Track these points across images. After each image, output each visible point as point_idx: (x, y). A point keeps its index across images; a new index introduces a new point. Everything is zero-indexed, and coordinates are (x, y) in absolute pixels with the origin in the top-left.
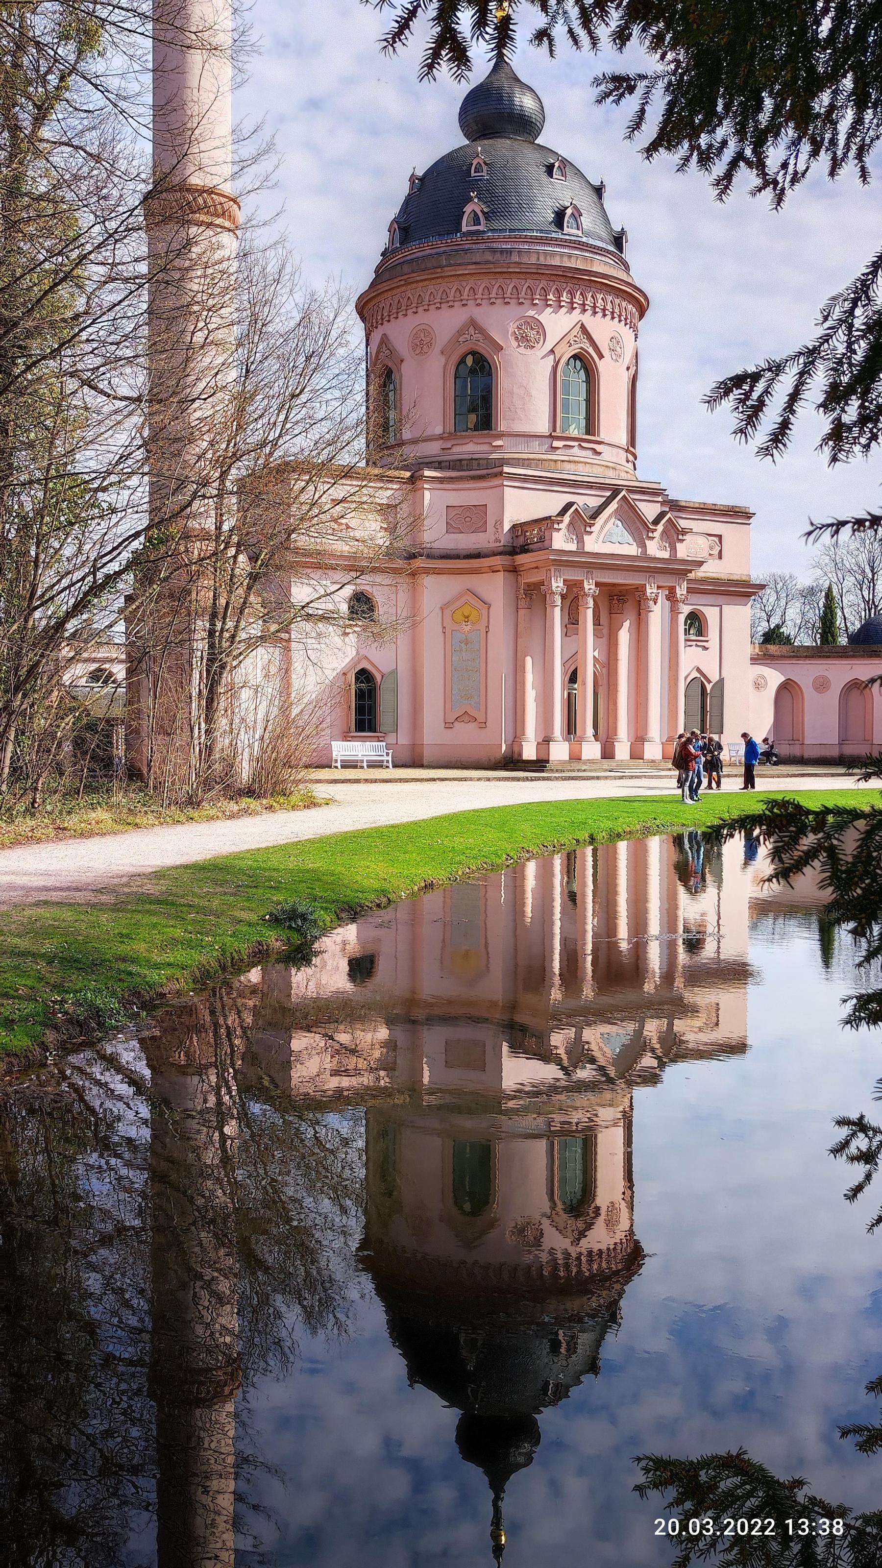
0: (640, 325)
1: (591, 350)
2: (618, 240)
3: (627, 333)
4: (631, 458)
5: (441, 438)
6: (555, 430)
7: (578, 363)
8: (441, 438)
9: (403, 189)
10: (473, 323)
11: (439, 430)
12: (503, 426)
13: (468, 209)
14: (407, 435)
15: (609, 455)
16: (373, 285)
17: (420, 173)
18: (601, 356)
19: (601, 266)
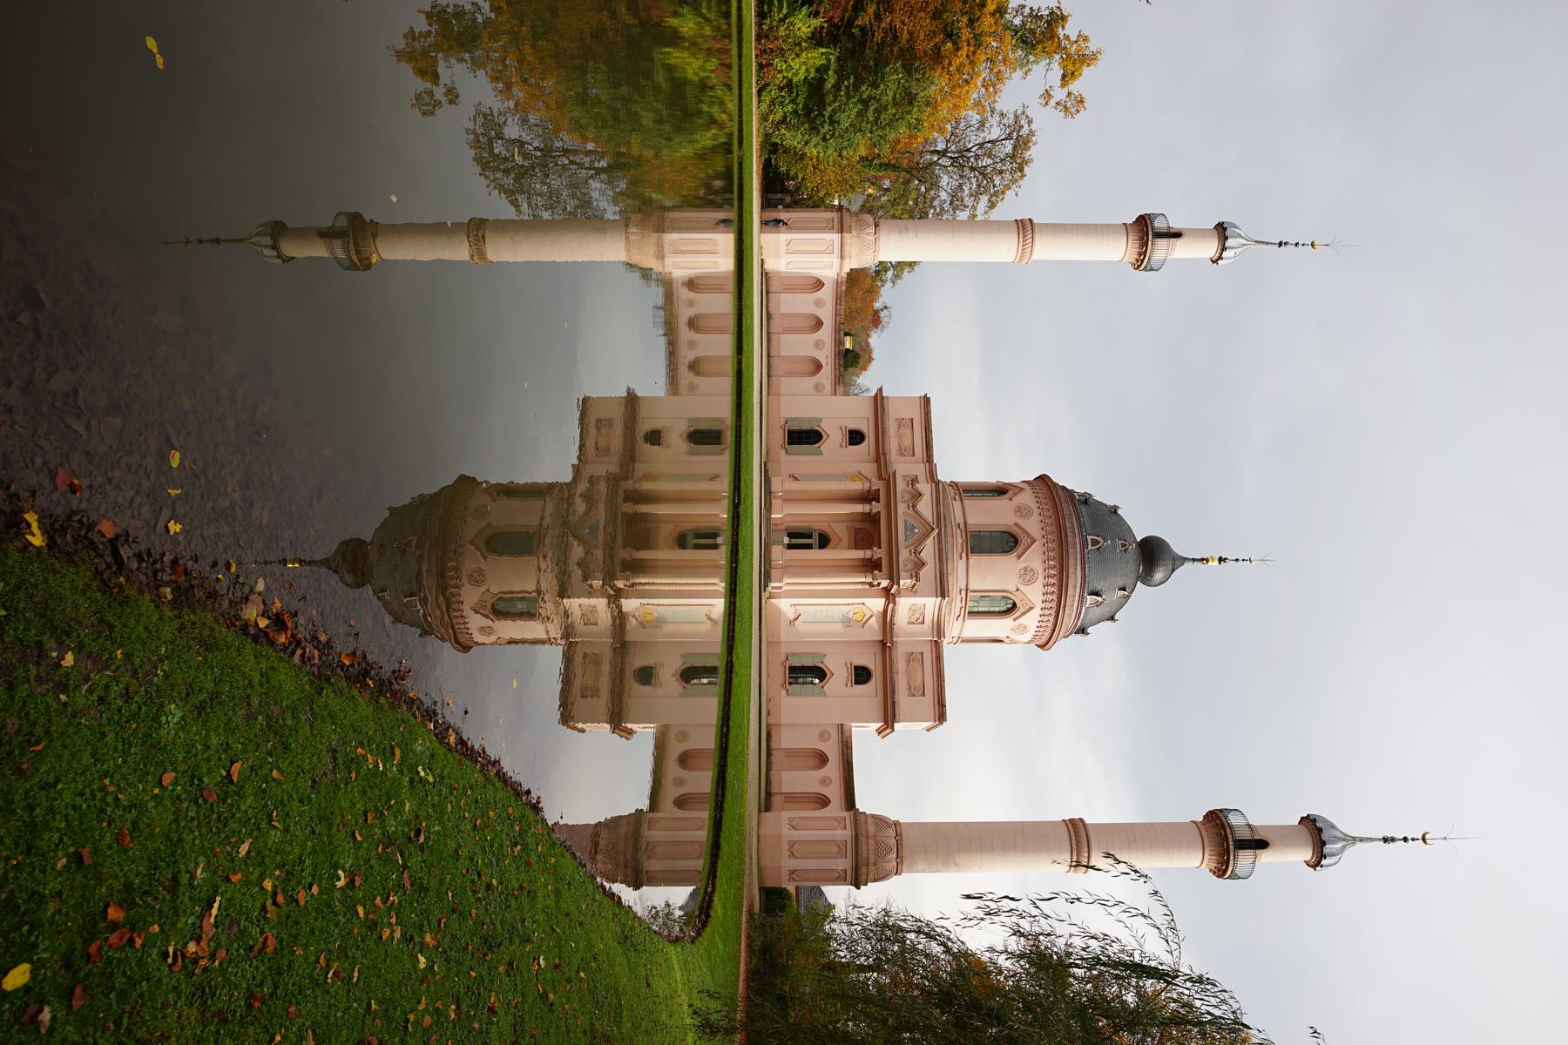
0: (1033, 645)
1: (1018, 614)
2: (1082, 631)
3: (1028, 636)
4: (955, 640)
5: (965, 523)
6: (972, 591)
7: (1010, 606)
8: (965, 523)
9: (1110, 503)
10: (1034, 541)
11: (970, 521)
12: (974, 559)
13: (1099, 539)
14: (967, 502)
15: (957, 625)
16: (1055, 485)
17: (1119, 511)
18: (1015, 620)
19: (1069, 620)
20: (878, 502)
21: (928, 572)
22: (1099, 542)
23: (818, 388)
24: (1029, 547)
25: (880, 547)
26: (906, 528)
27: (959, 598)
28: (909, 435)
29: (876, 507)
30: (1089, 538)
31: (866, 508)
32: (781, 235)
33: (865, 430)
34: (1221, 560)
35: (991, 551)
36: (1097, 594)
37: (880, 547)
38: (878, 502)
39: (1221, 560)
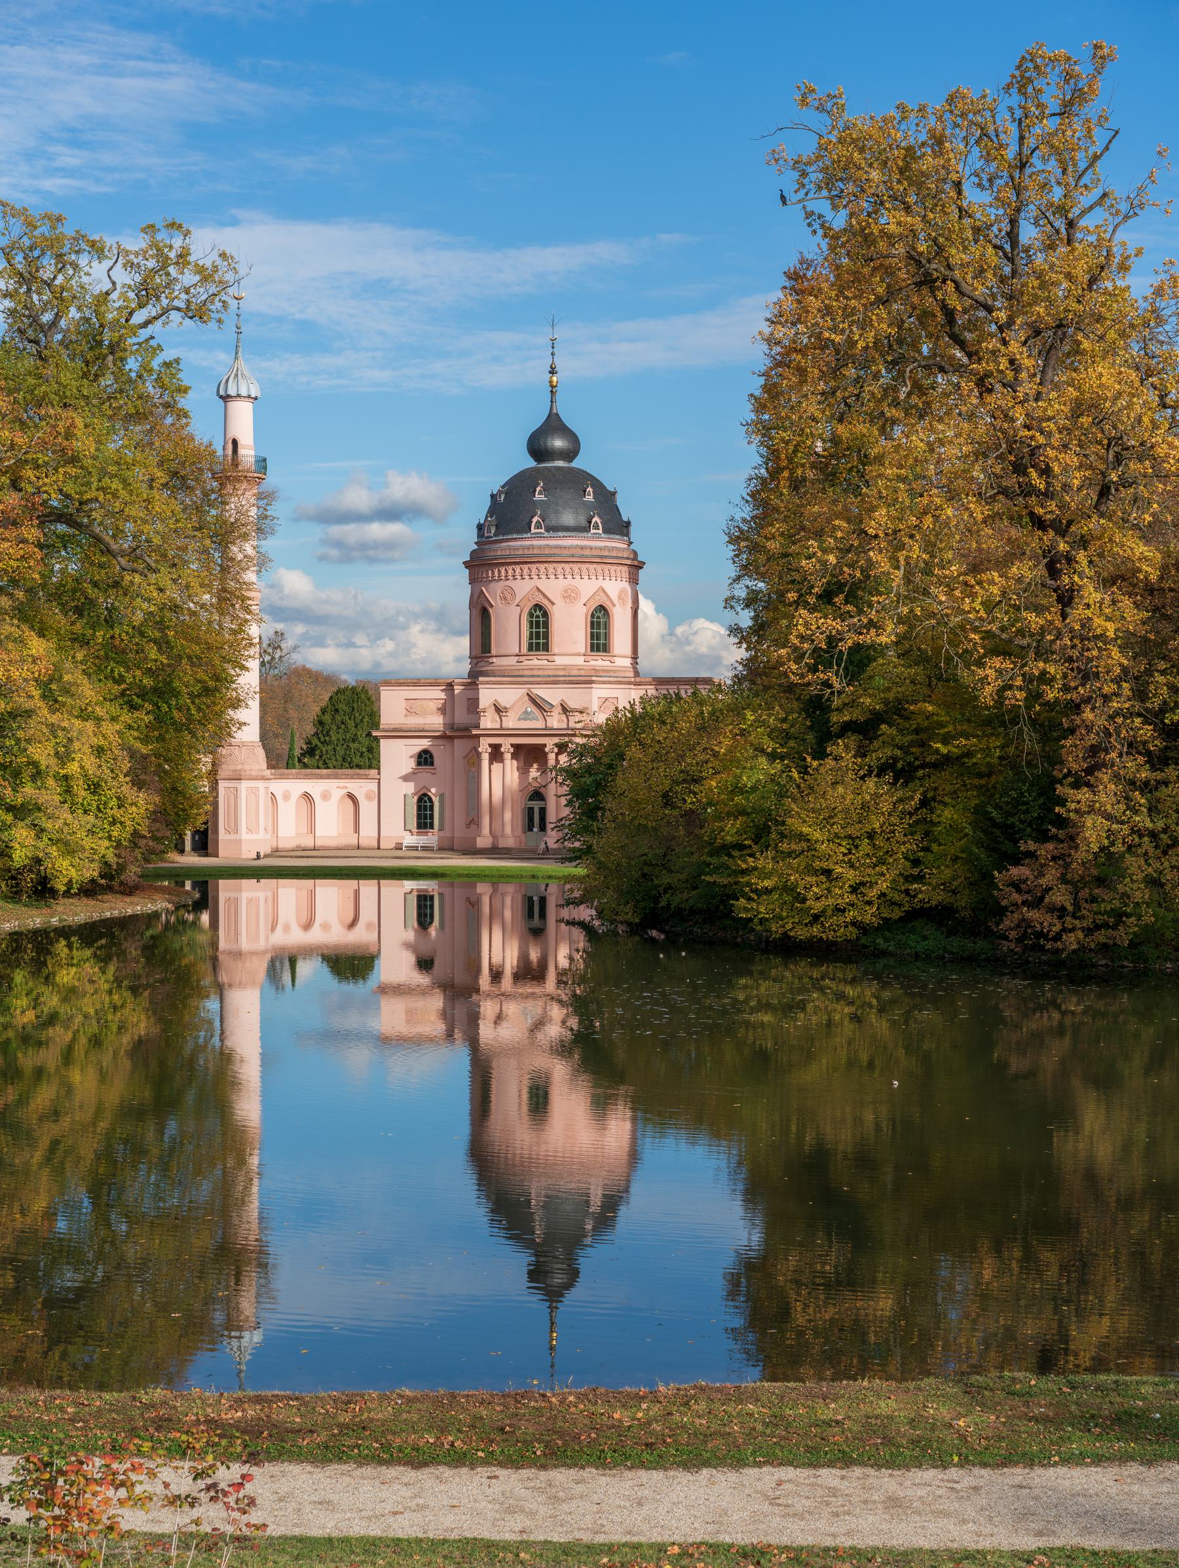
10: (538, 589)
11: (517, 651)
13: (535, 520)
20: (500, 746)
21: (573, 697)
22: (538, 522)
23: (368, 797)
24: (544, 595)
25: (545, 745)
26: (525, 719)
27: (592, 663)
28: (425, 702)
29: (506, 745)
30: (533, 531)
31: (508, 756)
32: (221, 837)
33: (418, 749)
34: (553, 371)
35: (546, 636)
36: (590, 522)
37: (545, 745)
38: (500, 746)
39: (553, 371)
